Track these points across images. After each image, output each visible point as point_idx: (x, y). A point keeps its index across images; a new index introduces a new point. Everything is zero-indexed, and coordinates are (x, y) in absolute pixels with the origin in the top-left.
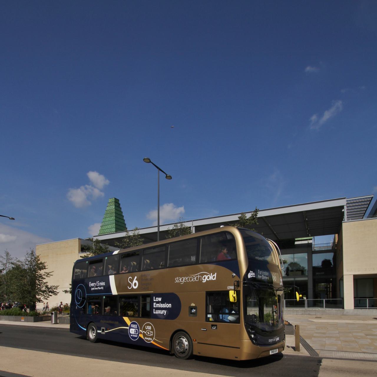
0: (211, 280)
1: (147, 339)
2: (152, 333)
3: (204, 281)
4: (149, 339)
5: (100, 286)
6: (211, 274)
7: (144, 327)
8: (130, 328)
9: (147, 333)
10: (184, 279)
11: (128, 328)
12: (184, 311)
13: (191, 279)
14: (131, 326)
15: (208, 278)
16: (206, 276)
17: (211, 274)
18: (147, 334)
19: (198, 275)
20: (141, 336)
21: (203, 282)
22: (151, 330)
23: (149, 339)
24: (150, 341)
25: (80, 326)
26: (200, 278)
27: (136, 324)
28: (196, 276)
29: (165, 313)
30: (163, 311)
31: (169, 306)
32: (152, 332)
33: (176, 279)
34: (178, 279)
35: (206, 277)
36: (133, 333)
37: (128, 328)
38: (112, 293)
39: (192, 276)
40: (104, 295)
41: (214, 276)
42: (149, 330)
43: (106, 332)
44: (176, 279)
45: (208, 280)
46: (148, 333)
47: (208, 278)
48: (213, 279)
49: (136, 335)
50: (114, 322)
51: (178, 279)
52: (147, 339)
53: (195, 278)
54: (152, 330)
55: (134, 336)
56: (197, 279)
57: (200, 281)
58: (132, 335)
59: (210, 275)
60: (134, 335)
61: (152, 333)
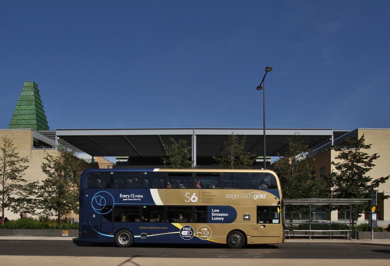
1: (203, 236)
2: (208, 233)
3: (255, 198)
4: (205, 237)
5: (137, 198)
6: (262, 194)
7: (200, 229)
8: (182, 230)
9: (203, 233)
10: (235, 196)
11: (179, 232)
12: (239, 217)
13: (242, 196)
14: (183, 229)
15: (259, 196)
16: (257, 195)
17: (262, 194)
18: (203, 234)
19: (249, 194)
20: (197, 236)
21: (254, 199)
22: (207, 231)
23: (205, 237)
24: (207, 238)
25: (99, 233)
26: (251, 196)
27: (189, 227)
29: (223, 219)
30: (221, 218)
31: (227, 215)
32: (208, 232)
33: (227, 196)
35: (257, 196)
36: (186, 234)
37: (179, 232)
38: (155, 203)
39: (244, 194)
40: (145, 205)
42: (205, 231)
43: (148, 236)
44: (227, 196)
46: (204, 233)
47: (259, 196)
48: (263, 198)
49: (190, 236)
50: (161, 228)
52: (203, 236)
53: (247, 196)
54: (209, 230)
55: (186, 236)
56: (248, 196)
58: (184, 236)
59: (261, 195)
60: (187, 235)
61: (208, 233)
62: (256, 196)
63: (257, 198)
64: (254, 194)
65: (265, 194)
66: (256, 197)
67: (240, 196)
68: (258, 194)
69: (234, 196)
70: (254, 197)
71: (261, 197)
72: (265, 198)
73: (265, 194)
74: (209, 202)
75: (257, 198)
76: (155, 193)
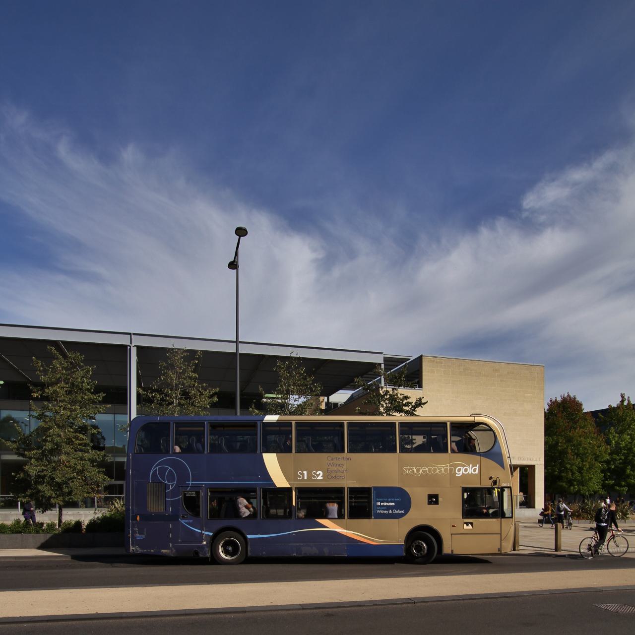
0: (470, 473)
3: (459, 474)
6: (471, 465)
15: (466, 470)
16: (462, 468)
17: (471, 465)
21: (457, 475)
26: (451, 470)
28: (444, 467)
33: (406, 469)
34: (410, 469)
35: (463, 470)
38: (270, 479)
39: (438, 467)
41: (476, 469)
44: (406, 469)
45: (464, 473)
47: (466, 470)
51: (410, 469)
53: (443, 470)
56: (446, 470)
57: (452, 475)
62: (459, 470)
63: (463, 473)
64: (455, 466)
65: (478, 465)
66: (460, 471)
67: (430, 470)
68: (464, 466)
69: (418, 470)
70: (457, 473)
71: (470, 470)
72: (477, 472)
73: (478, 465)
74: (338, 478)
75: (463, 473)
76: (271, 460)
